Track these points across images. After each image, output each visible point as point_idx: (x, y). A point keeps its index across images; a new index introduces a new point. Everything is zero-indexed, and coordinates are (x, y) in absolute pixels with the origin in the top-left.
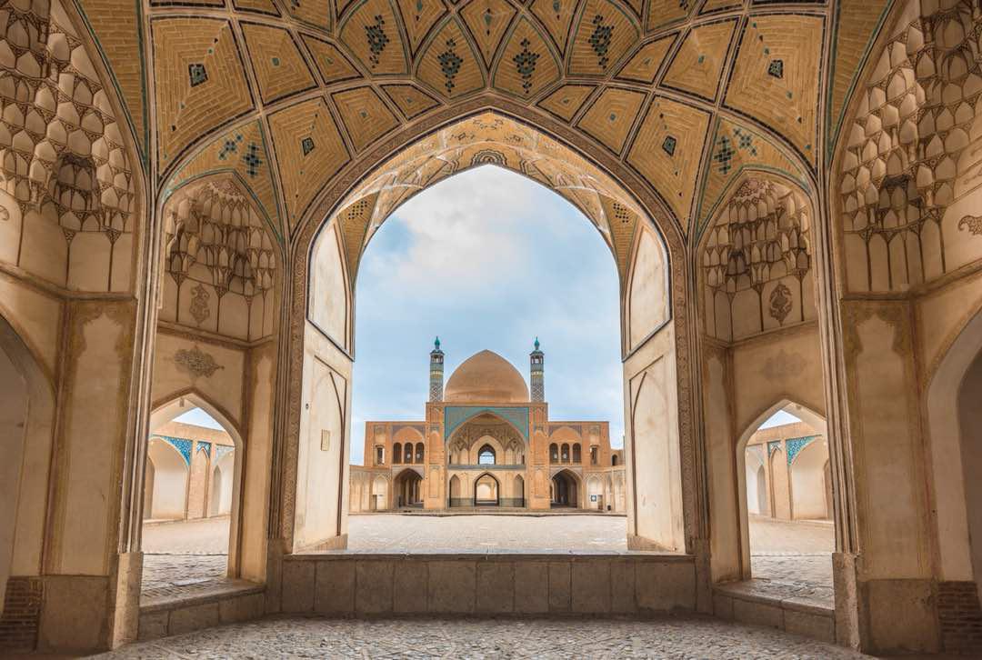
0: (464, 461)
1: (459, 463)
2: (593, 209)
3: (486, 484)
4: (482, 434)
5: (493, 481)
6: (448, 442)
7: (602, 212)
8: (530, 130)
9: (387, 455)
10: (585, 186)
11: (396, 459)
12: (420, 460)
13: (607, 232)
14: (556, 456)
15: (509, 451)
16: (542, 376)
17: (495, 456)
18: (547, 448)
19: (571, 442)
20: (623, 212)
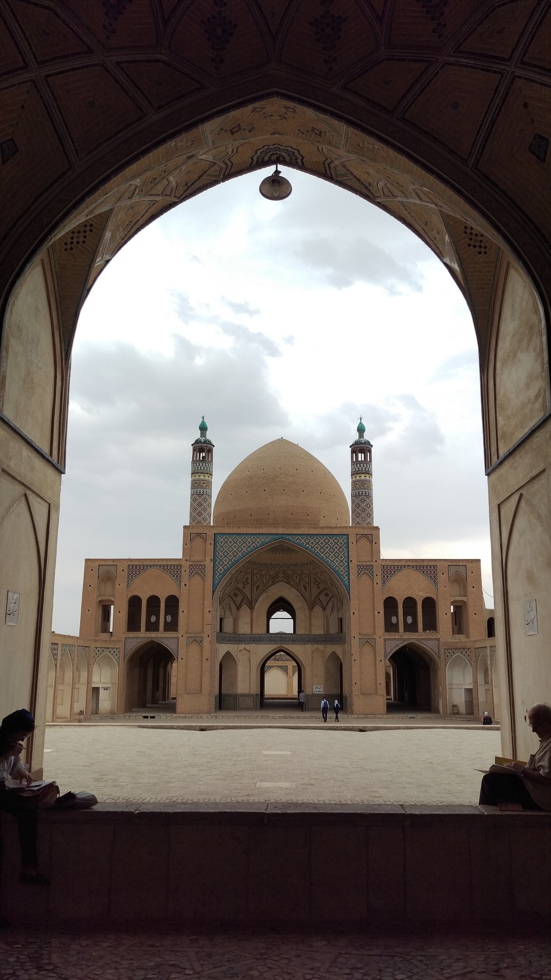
0: (244, 629)
1: (235, 632)
2: (435, 233)
3: (281, 667)
4: (274, 580)
5: (291, 664)
6: (218, 594)
7: (447, 238)
8: (336, 123)
10: (421, 199)
11: (133, 624)
12: (172, 626)
13: (456, 267)
14: (394, 620)
15: (318, 609)
16: (370, 482)
17: (294, 618)
18: (380, 607)
19: (419, 596)
20: (479, 238)
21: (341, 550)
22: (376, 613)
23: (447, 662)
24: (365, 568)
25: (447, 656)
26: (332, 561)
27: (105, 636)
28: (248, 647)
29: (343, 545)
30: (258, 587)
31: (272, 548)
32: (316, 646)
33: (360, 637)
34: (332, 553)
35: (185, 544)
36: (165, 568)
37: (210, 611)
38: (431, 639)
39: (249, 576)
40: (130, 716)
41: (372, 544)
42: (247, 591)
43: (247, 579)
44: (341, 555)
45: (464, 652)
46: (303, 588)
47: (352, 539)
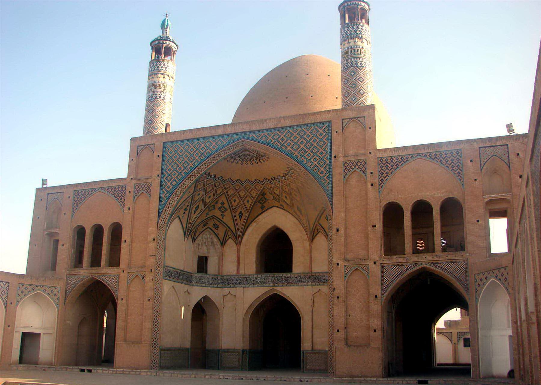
0: (230, 269)
9: (66, 252)
12: (114, 262)
15: (320, 239)
19: (435, 197)
21: (321, 143)
22: (370, 227)
23: (479, 295)
24: (355, 164)
25: (479, 285)
26: (309, 161)
27: (50, 273)
28: (233, 291)
29: (324, 137)
30: (241, 215)
31: (234, 154)
32: (316, 288)
33: (346, 263)
34: (308, 149)
35: (131, 159)
36: (110, 190)
37: (154, 240)
38: (455, 261)
39: (223, 199)
40: (67, 369)
41: (364, 131)
42: (228, 219)
43: (223, 203)
44: (322, 150)
45: (499, 276)
46: (298, 213)
47: (337, 126)
